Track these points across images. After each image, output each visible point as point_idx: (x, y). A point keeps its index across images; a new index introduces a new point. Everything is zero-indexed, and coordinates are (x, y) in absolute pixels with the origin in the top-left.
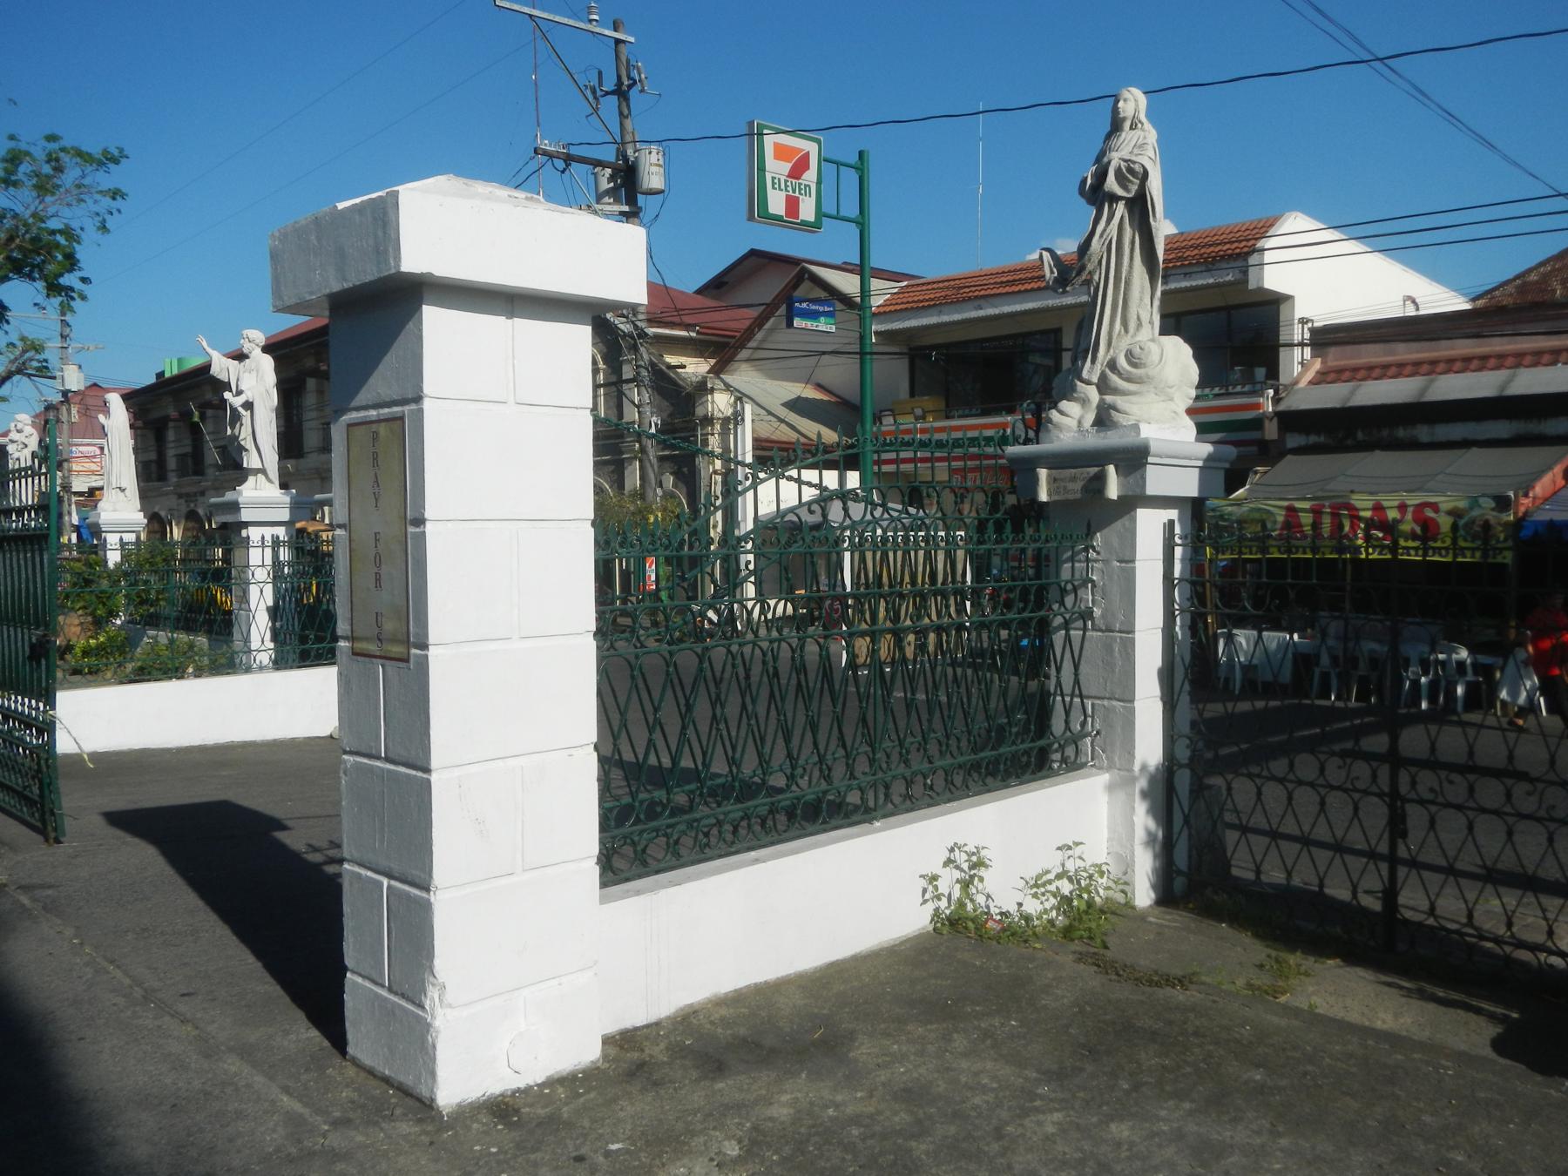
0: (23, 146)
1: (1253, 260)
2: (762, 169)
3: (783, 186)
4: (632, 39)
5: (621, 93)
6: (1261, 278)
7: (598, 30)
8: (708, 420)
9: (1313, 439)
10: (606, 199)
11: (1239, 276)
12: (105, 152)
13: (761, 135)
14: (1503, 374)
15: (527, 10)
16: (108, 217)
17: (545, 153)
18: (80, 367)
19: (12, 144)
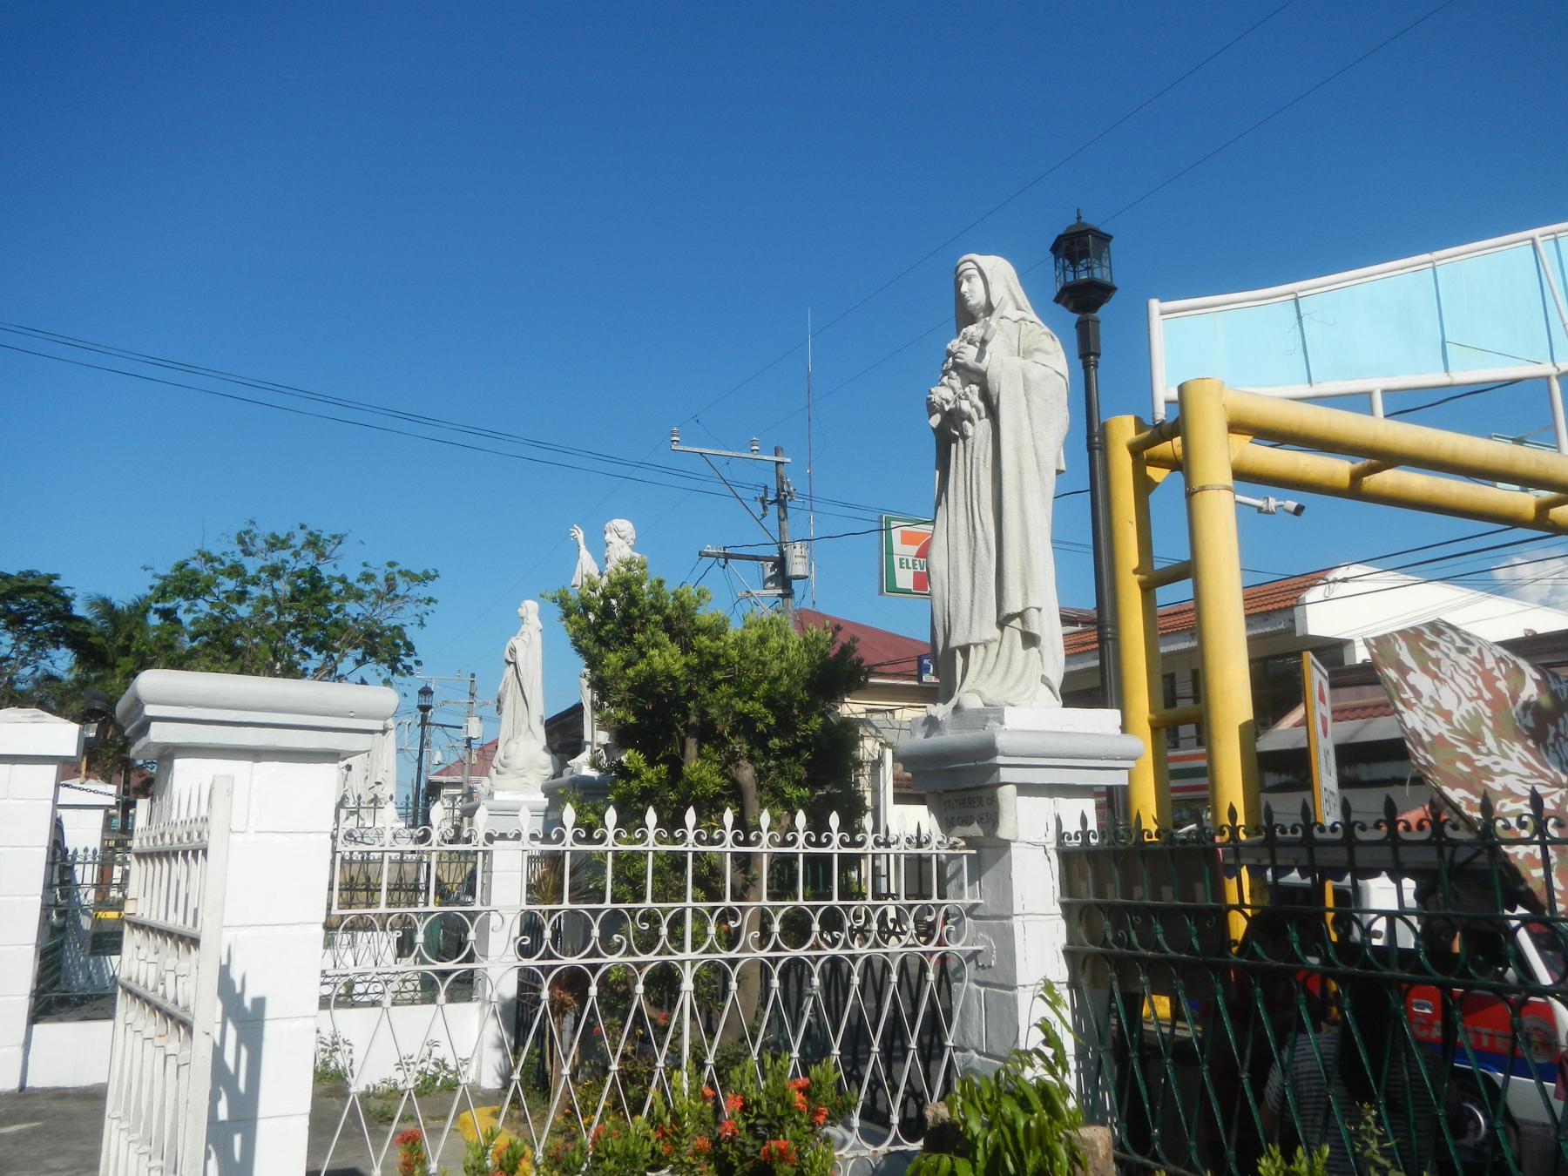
0: (371, 571)
1: (1297, 610)
2: (890, 553)
3: (911, 565)
4: (789, 460)
5: (781, 502)
6: (1305, 627)
7: (758, 457)
8: (859, 764)
9: (1284, 778)
10: (769, 585)
11: (1289, 624)
12: (426, 573)
13: (889, 529)
14: (1359, 722)
15: (697, 450)
16: (425, 616)
17: (708, 555)
18: (481, 719)
19: (365, 569)
